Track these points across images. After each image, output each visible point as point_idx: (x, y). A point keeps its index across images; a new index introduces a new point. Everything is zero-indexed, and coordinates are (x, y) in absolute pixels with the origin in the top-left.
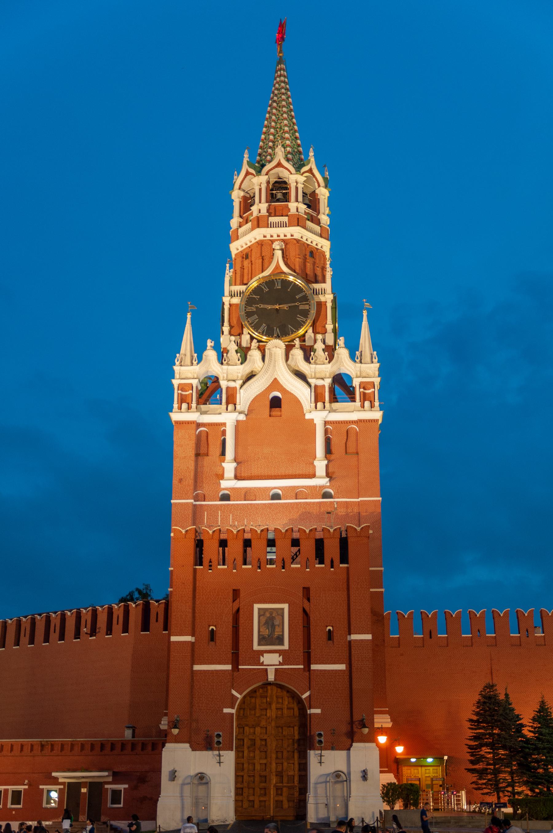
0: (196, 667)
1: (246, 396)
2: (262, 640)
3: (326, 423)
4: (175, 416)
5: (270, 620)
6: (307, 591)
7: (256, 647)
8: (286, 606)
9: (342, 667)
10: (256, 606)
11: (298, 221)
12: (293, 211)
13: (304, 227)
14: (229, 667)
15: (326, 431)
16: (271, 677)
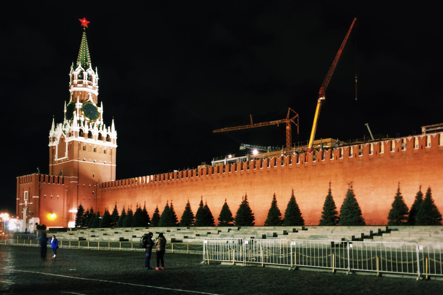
1: (58, 138)
3: (69, 142)
7: (25, 200)
10: (25, 192)
16: (26, 205)
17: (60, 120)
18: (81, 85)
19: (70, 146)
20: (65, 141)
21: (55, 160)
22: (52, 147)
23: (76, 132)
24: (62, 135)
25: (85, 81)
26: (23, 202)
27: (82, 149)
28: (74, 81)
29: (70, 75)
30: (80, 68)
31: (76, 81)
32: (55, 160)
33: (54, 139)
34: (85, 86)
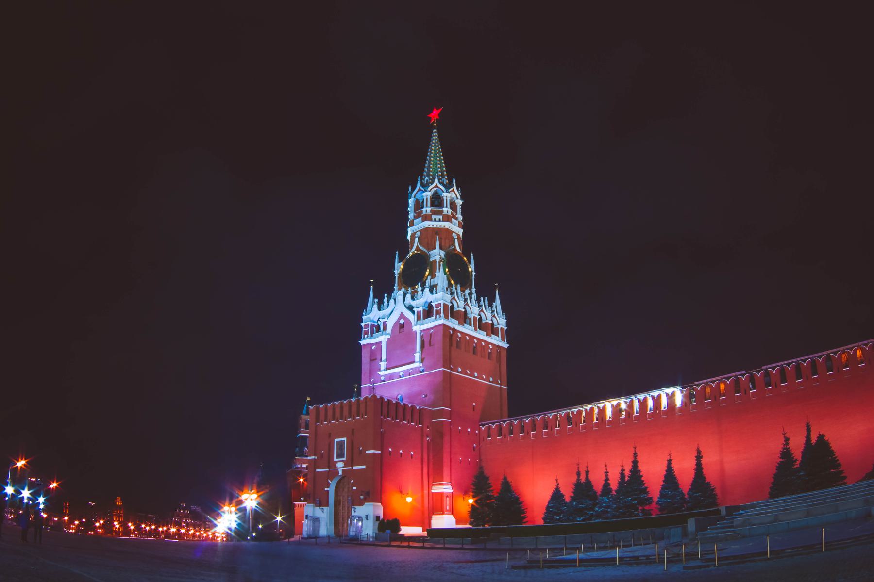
0: (318, 470)
2: (339, 456)
3: (422, 331)
4: (362, 342)
5: (340, 444)
6: (353, 430)
7: (335, 460)
8: (345, 439)
9: (364, 467)
10: (336, 440)
11: (427, 218)
12: (424, 213)
13: (430, 220)
14: (327, 469)
15: (422, 337)
16: (340, 473)
17: (384, 291)
18: (441, 217)
19: (427, 340)
20: (414, 328)
21: (380, 373)
22: (371, 345)
23: (445, 305)
24: (402, 316)
25: (447, 210)
26: (331, 464)
27: (454, 344)
28: (424, 210)
29: (411, 201)
30: (436, 186)
31: (427, 210)
32: (380, 373)
33: (377, 329)
34: (447, 218)
